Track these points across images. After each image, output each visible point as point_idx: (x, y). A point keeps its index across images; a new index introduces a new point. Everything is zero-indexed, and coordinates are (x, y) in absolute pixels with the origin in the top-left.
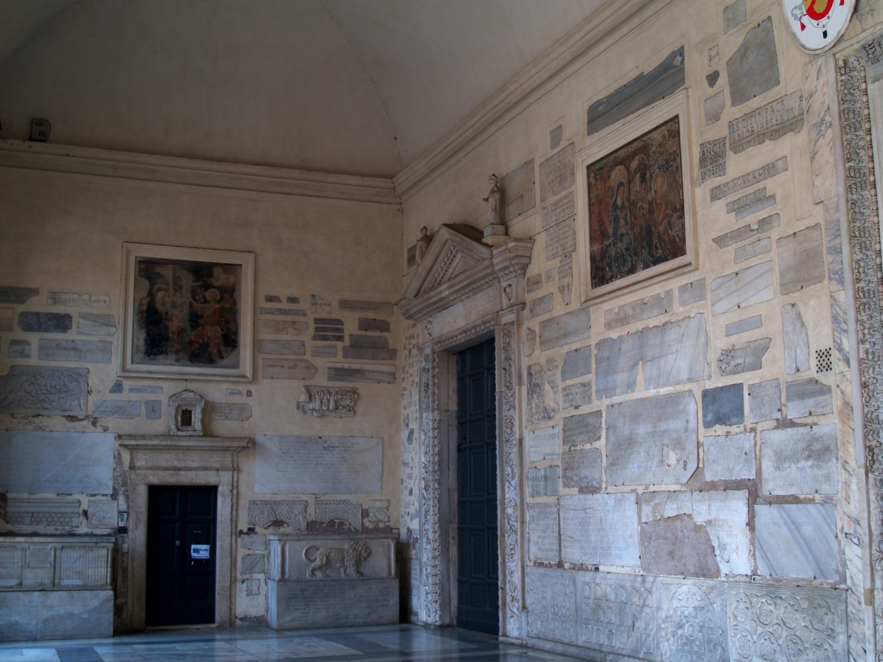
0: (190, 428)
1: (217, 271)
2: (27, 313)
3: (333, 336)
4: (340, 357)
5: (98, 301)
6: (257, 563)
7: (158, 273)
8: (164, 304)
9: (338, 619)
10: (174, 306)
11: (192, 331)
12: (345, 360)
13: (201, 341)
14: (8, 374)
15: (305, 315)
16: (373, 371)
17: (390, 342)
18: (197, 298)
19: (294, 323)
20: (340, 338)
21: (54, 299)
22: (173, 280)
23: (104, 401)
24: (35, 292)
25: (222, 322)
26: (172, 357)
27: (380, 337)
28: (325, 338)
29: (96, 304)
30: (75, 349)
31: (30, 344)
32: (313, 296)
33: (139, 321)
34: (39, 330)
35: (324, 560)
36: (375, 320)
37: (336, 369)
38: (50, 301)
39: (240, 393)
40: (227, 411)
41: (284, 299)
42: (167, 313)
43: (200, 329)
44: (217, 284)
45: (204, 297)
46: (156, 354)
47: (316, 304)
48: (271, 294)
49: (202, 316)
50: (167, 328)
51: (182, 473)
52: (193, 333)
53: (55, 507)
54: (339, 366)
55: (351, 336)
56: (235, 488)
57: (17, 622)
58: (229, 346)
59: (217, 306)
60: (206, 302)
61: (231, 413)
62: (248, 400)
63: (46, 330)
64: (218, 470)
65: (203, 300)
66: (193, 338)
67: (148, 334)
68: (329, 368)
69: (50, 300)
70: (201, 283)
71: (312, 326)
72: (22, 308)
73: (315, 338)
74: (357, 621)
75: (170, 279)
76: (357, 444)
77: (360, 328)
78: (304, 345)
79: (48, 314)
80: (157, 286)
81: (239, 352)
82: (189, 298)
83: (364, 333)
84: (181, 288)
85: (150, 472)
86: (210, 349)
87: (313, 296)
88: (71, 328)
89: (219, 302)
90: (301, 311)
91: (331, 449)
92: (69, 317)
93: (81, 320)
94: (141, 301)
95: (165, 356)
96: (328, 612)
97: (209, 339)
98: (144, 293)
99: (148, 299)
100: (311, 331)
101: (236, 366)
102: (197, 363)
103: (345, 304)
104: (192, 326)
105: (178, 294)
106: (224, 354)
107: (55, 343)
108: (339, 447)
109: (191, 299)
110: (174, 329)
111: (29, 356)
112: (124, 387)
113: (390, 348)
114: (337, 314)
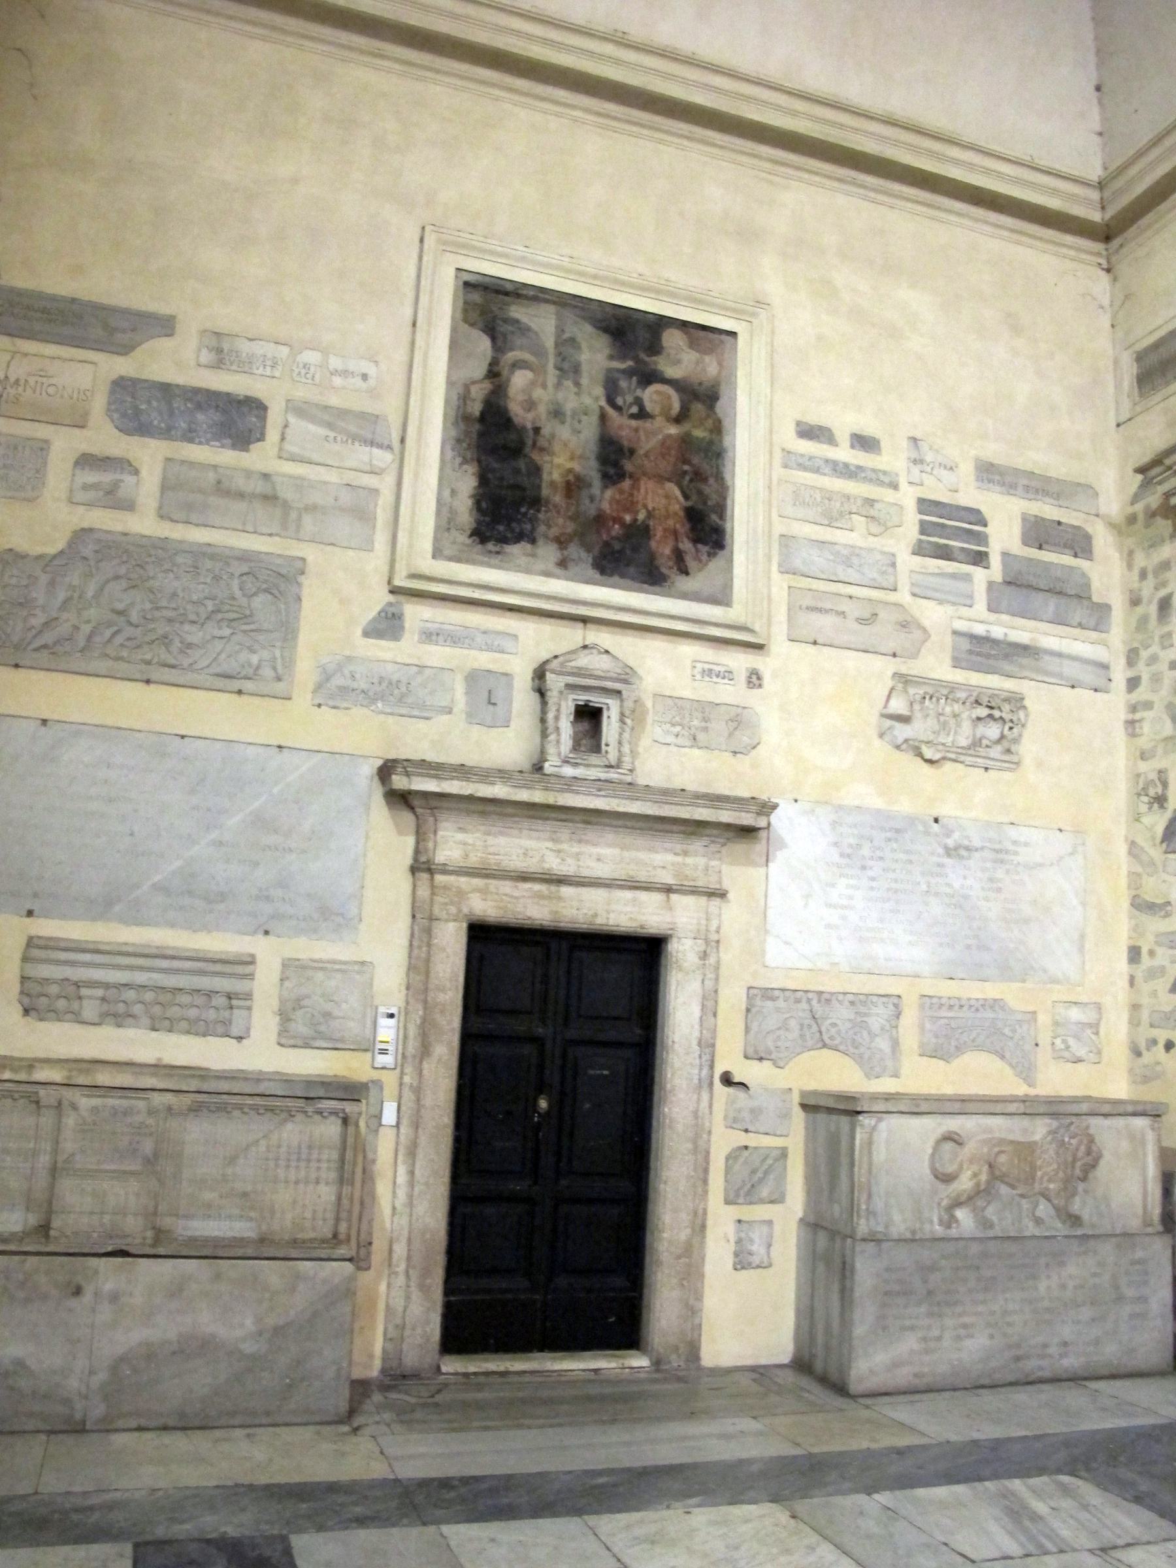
0: (594, 759)
1: (672, 339)
2: (135, 382)
3: (963, 549)
4: (981, 606)
5: (345, 373)
6: (766, 1173)
7: (517, 321)
8: (531, 405)
9: (1018, 1359)
10: (557, 413)
11: (605, 487)
12: (993, 617)
13: (628, 518)
14: (62, 552)
15: (895, 486)
16: (1060, 655)
17: (1096, 584)
18: (619, 401)
19: (870, 502)
20: (980, 559)
21: (219, 351)
22: (557, 345)
23: (349, 659)
24: (165, 325)
25: (685, 473)
26: (548, 553)
27: (1071, 568)
28: (944, 554)
29: (338, 381)
30: (270, 499)
31: (136, 472)
32: (914, 440)
33: (458, 441)
34: (167, 433)
35: (984, 1177)
36: (1059, 523)
37: (973, 637)
38: (206, 357)
39: (728, 675)
40: (696, 723)
41: (843, 435)
42: (537, 430)
43: (626, 484)
44: (671, 372)
45: (639, 402)
46: (503, 540)
47: (922, 462)
48: (813, 419)
49: (632, 452)
50: (536, 470)
51: (566, 891)
52: (609, 493)
53: (177, 971)
54: (979, 629)
55: (1005, 555)
56: (710, 944)
57: (20, 1364)
58: (705, 543)
59: (673, 430)
60: (643, 414)
61: (706, 729)
62: (753, 698)
63: (190, 436)
64: (668, 890)
65: (634, 410)
66: (606, 506)
67: (483, 479)
68: (955, 633)
69: (204, 351)
70: (630, 363)
71: (912, 518)
72: (123, 366)
73: (920, 550)
74: (1066, 1362)
75: (549, 343)
76: (1026, 844)
77: (1026, 542)
78: (894, 565)
79: (197, 391)
80: (511, 356)
81: (730, 561)
82: (597, 399)
83: (1034, 553)
84: (576, 369)
85: (478, 882)
86: (653, 544)
87: (914, 440)
88: (262, 438)
89: (678, 420)
90: (885, 473)
91: (964, 853)
92: (255, 406)
93: (292, 420)
94: (467, 387)
95: (529, 546)
96: (992, 1337)
97: (650, 515)
98: (478, 369)
99: (487, 386)
100: (910, 530)
101: (722, 598)
102: (616, 579)
103: (989, 472)
104: (605, 476)
105: (568, 383)
106: (691, 563)
107: (211, 476)
108: (982, 848)
109: (603, 403)
110: (556, 476)
111: (129, 506)
112: (407, 625)
113: (1095, 599)
114: (970, 495)
